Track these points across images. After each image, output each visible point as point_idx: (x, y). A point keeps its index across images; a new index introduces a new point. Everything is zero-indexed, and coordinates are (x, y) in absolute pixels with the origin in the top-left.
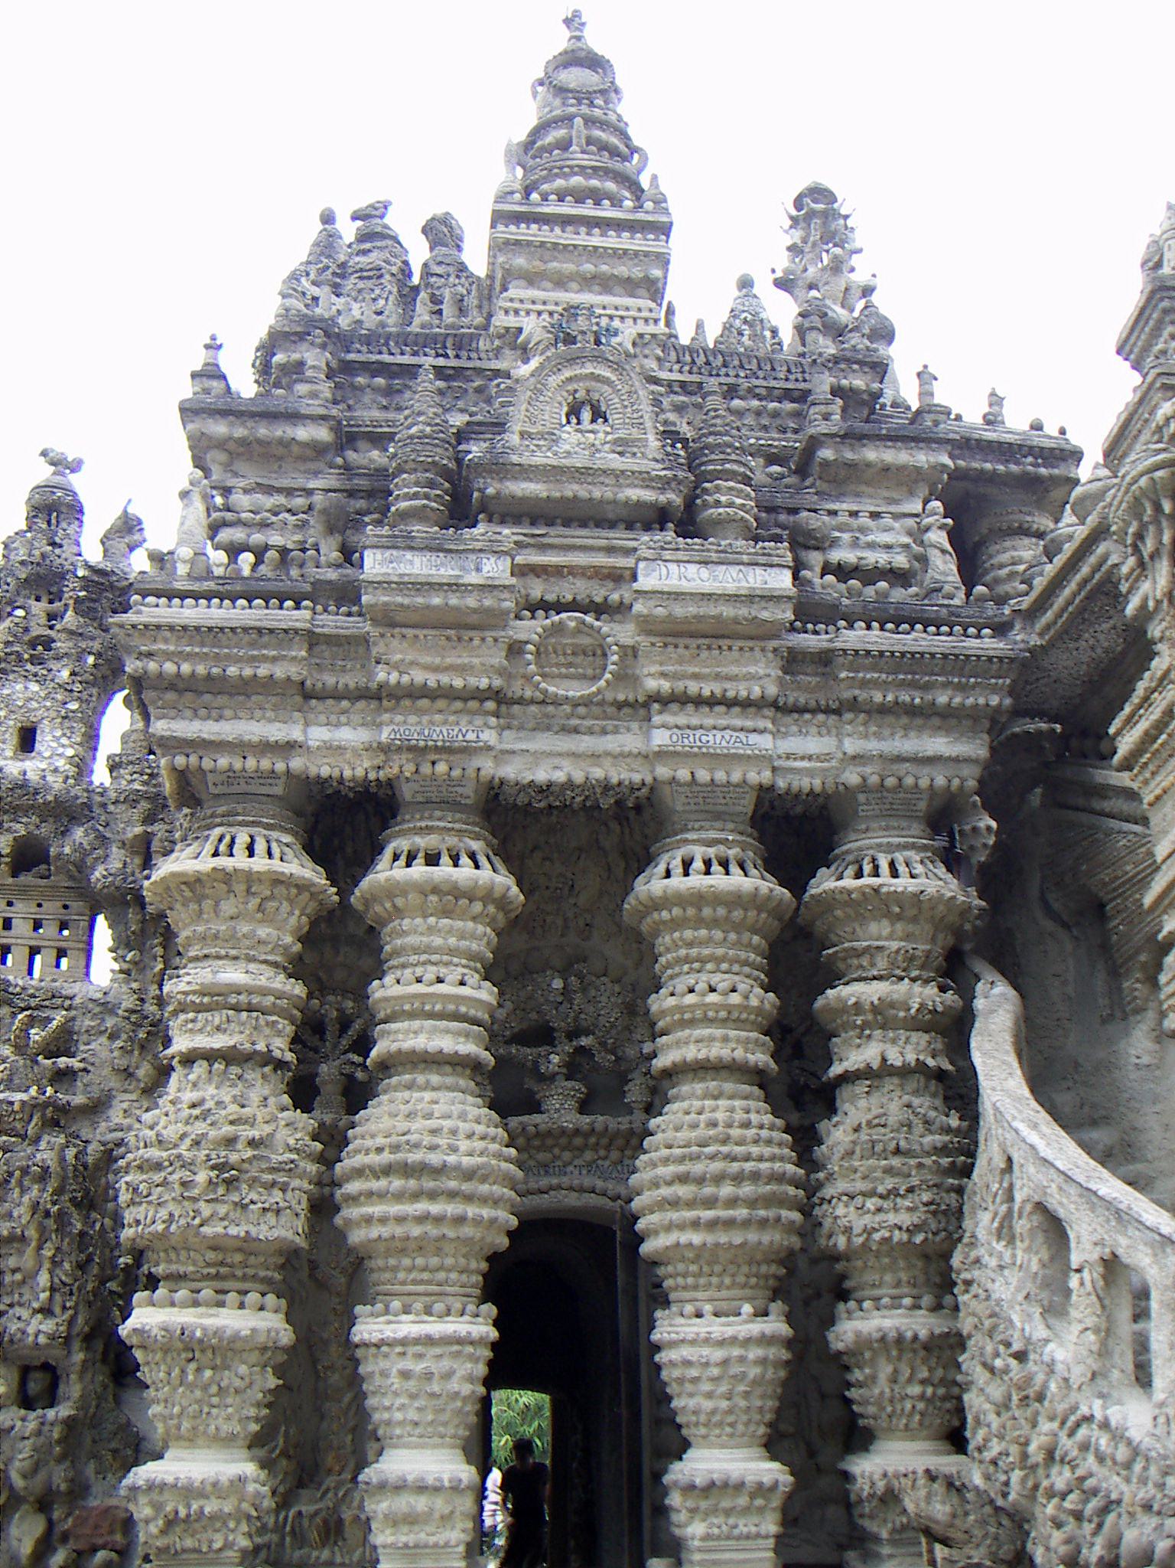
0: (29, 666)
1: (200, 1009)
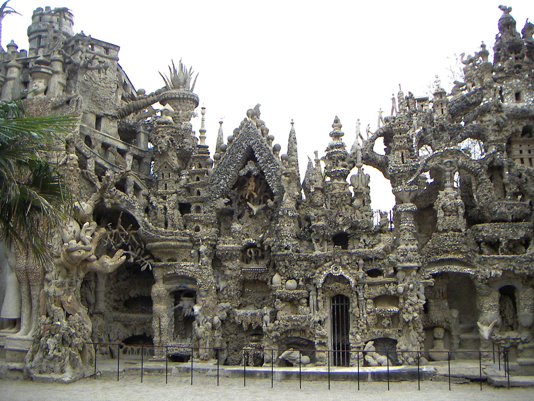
0: (516, 75)
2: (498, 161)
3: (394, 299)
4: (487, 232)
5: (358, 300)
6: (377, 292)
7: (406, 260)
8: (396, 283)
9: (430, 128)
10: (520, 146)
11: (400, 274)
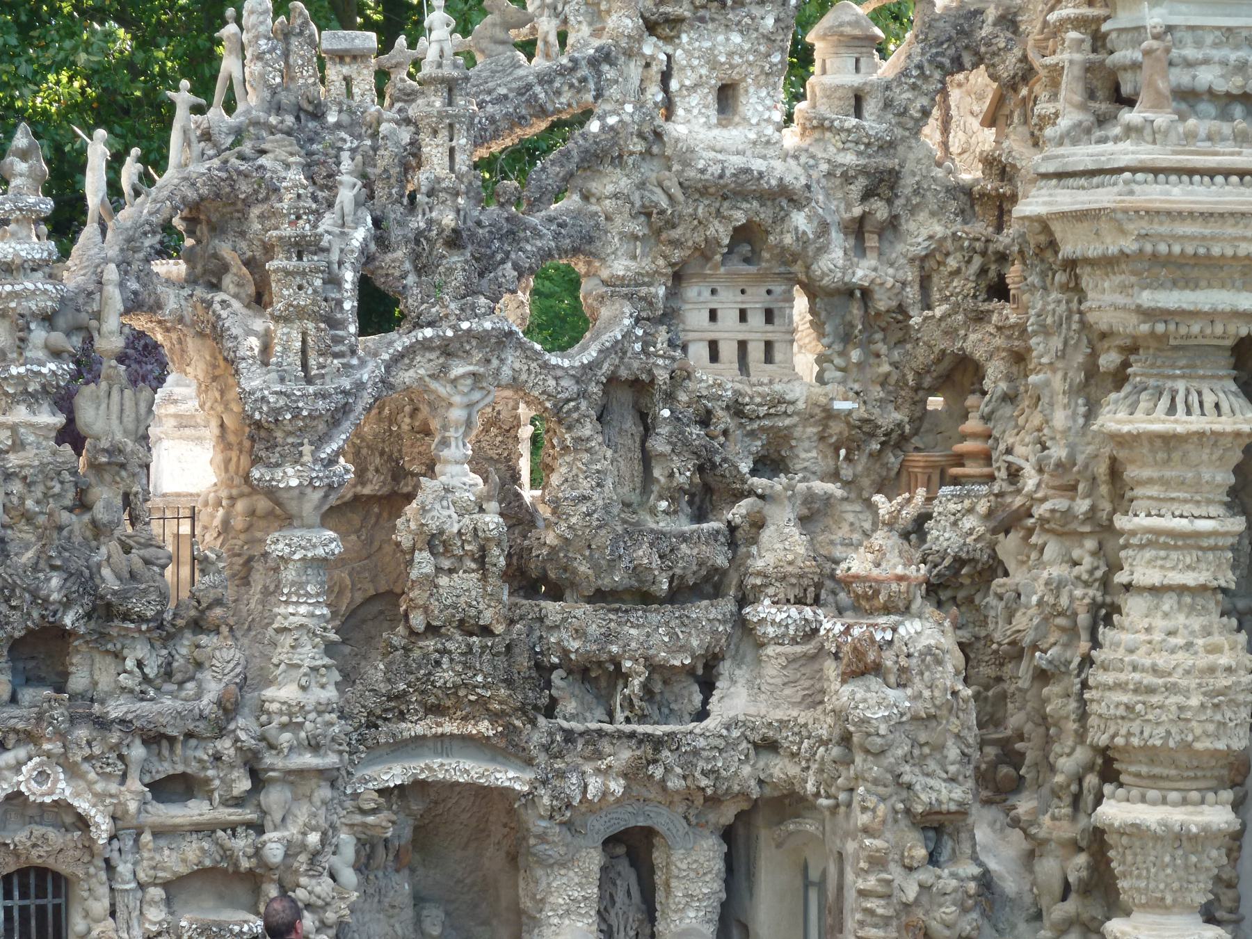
1: (1166, 546)
2: (636, 364)
4: (579, 633)
5: (112, 889)
6: (184, 861)
7: (300, 744)
8: (259, 829)
9: (401, 224)
10: (713, 292)
11: (274, 798)
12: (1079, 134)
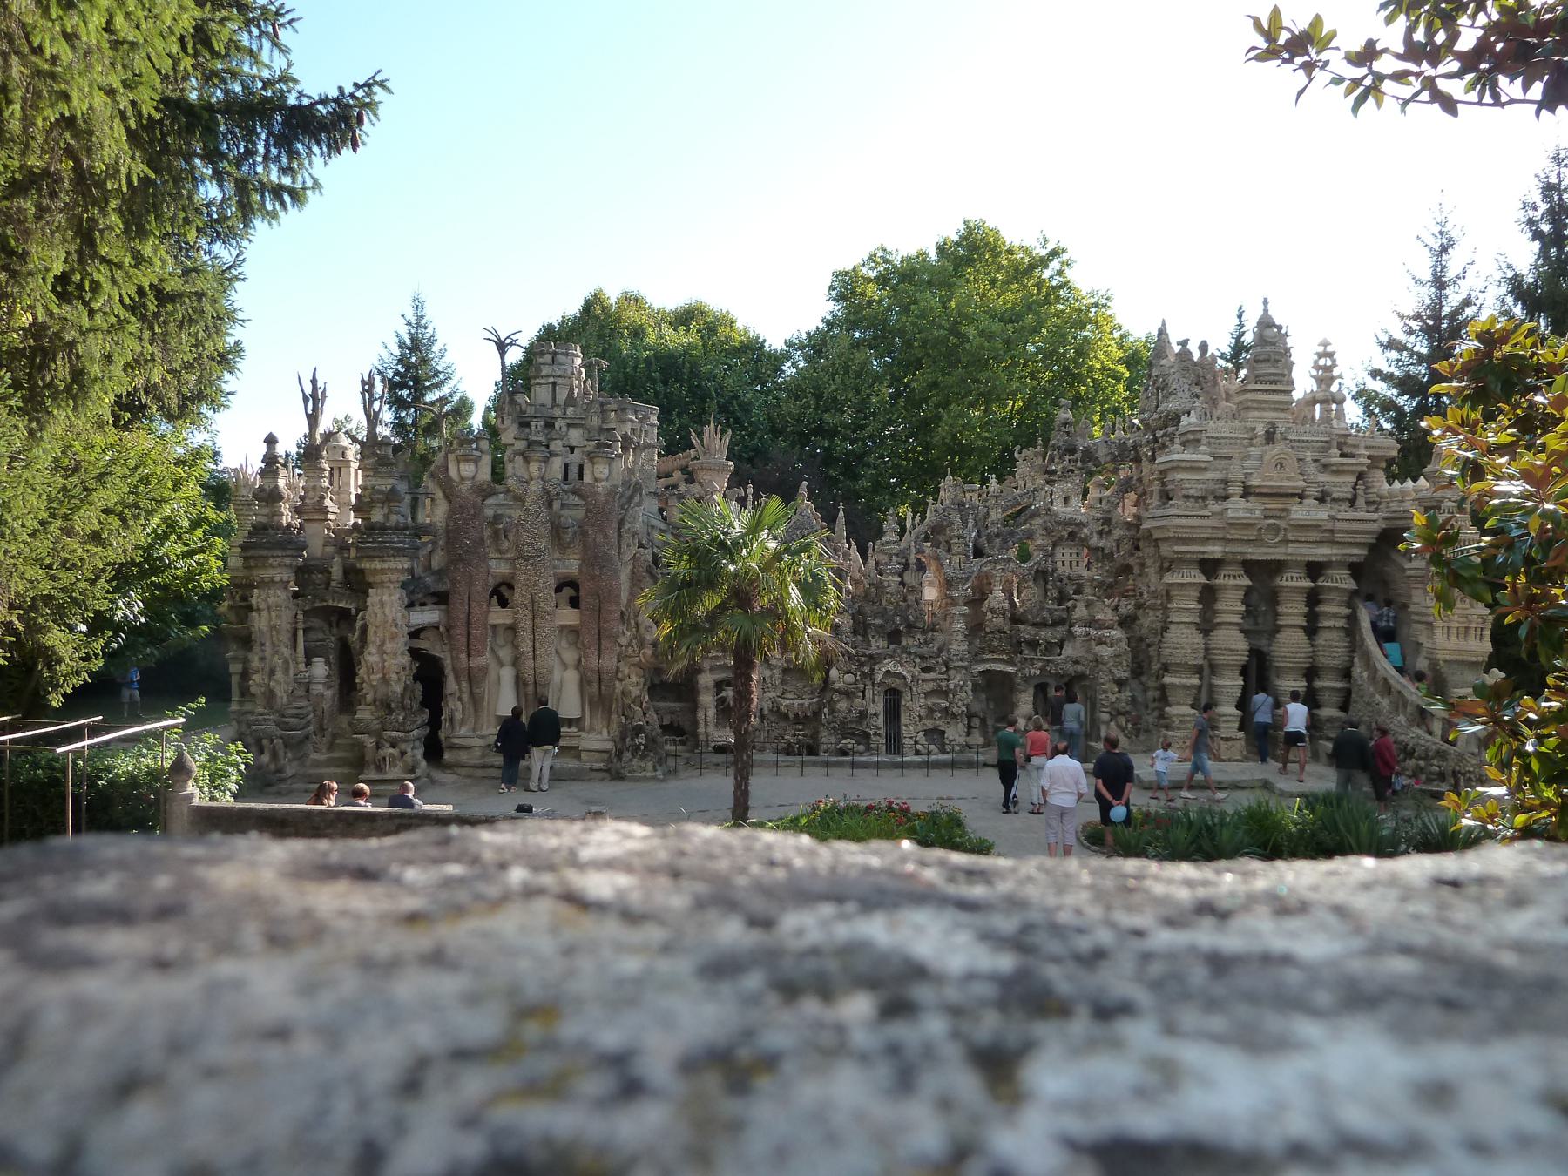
3: (944, 693)
11: (952, 672)
12: (1158, 507)
